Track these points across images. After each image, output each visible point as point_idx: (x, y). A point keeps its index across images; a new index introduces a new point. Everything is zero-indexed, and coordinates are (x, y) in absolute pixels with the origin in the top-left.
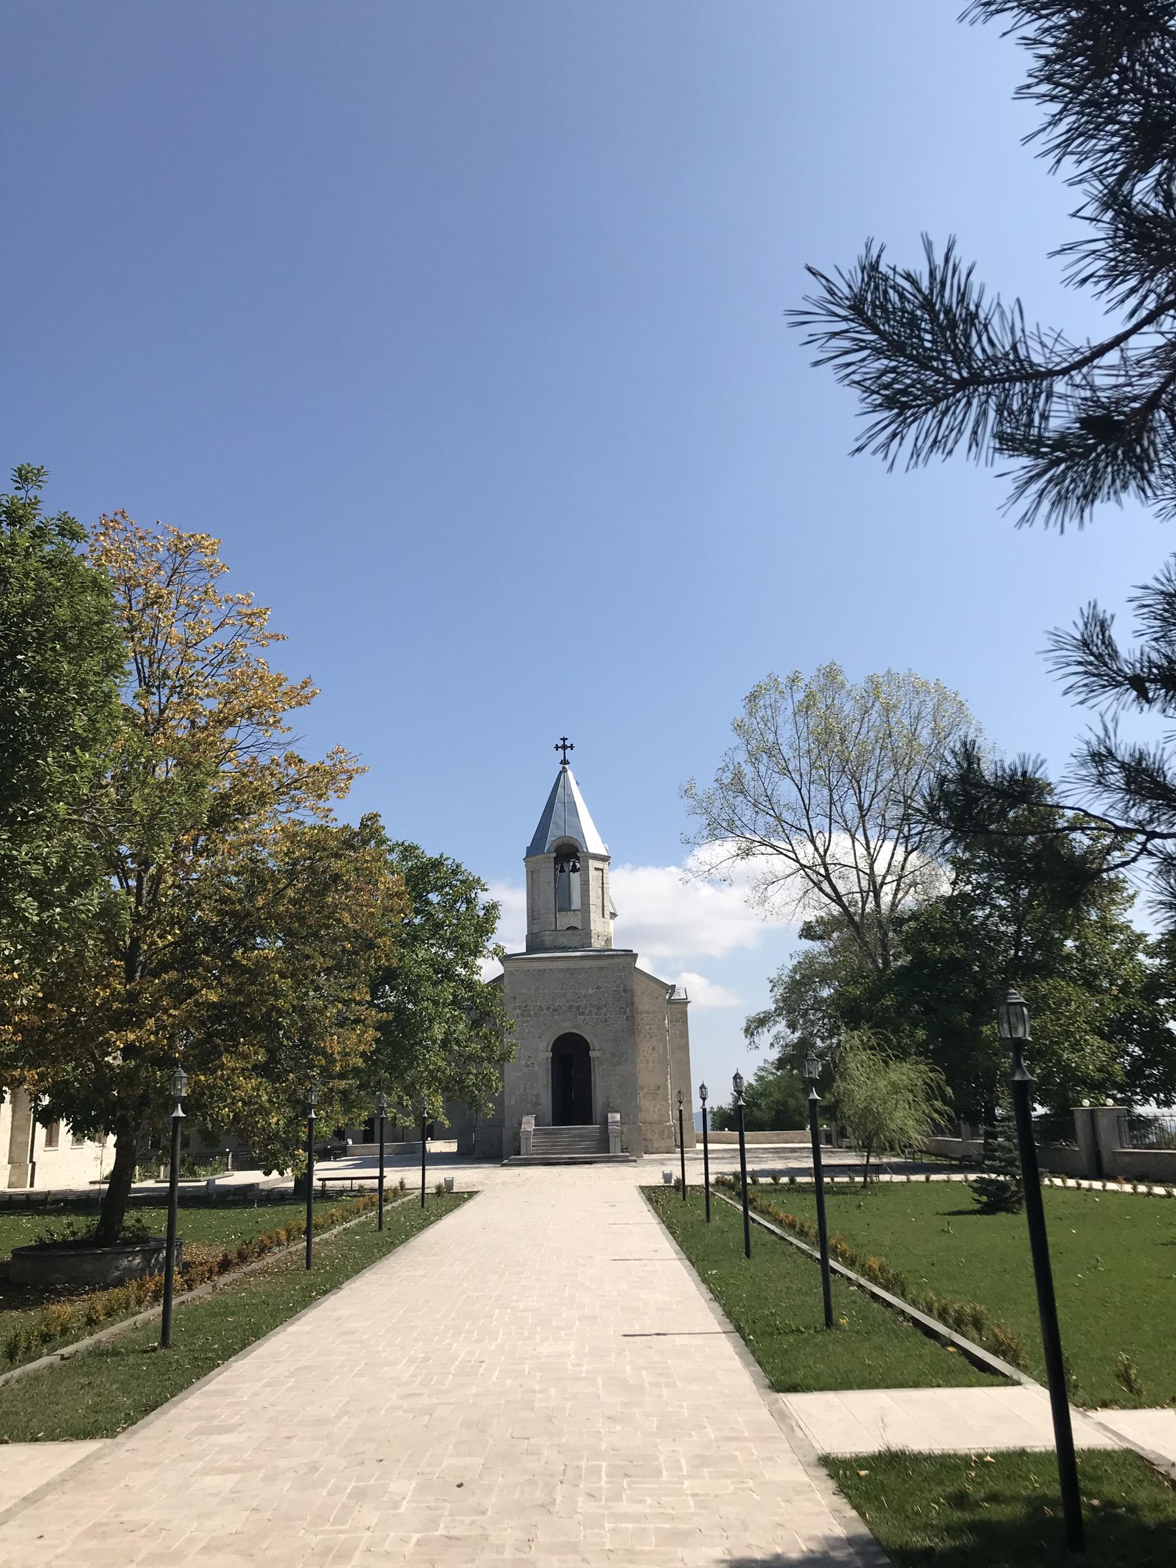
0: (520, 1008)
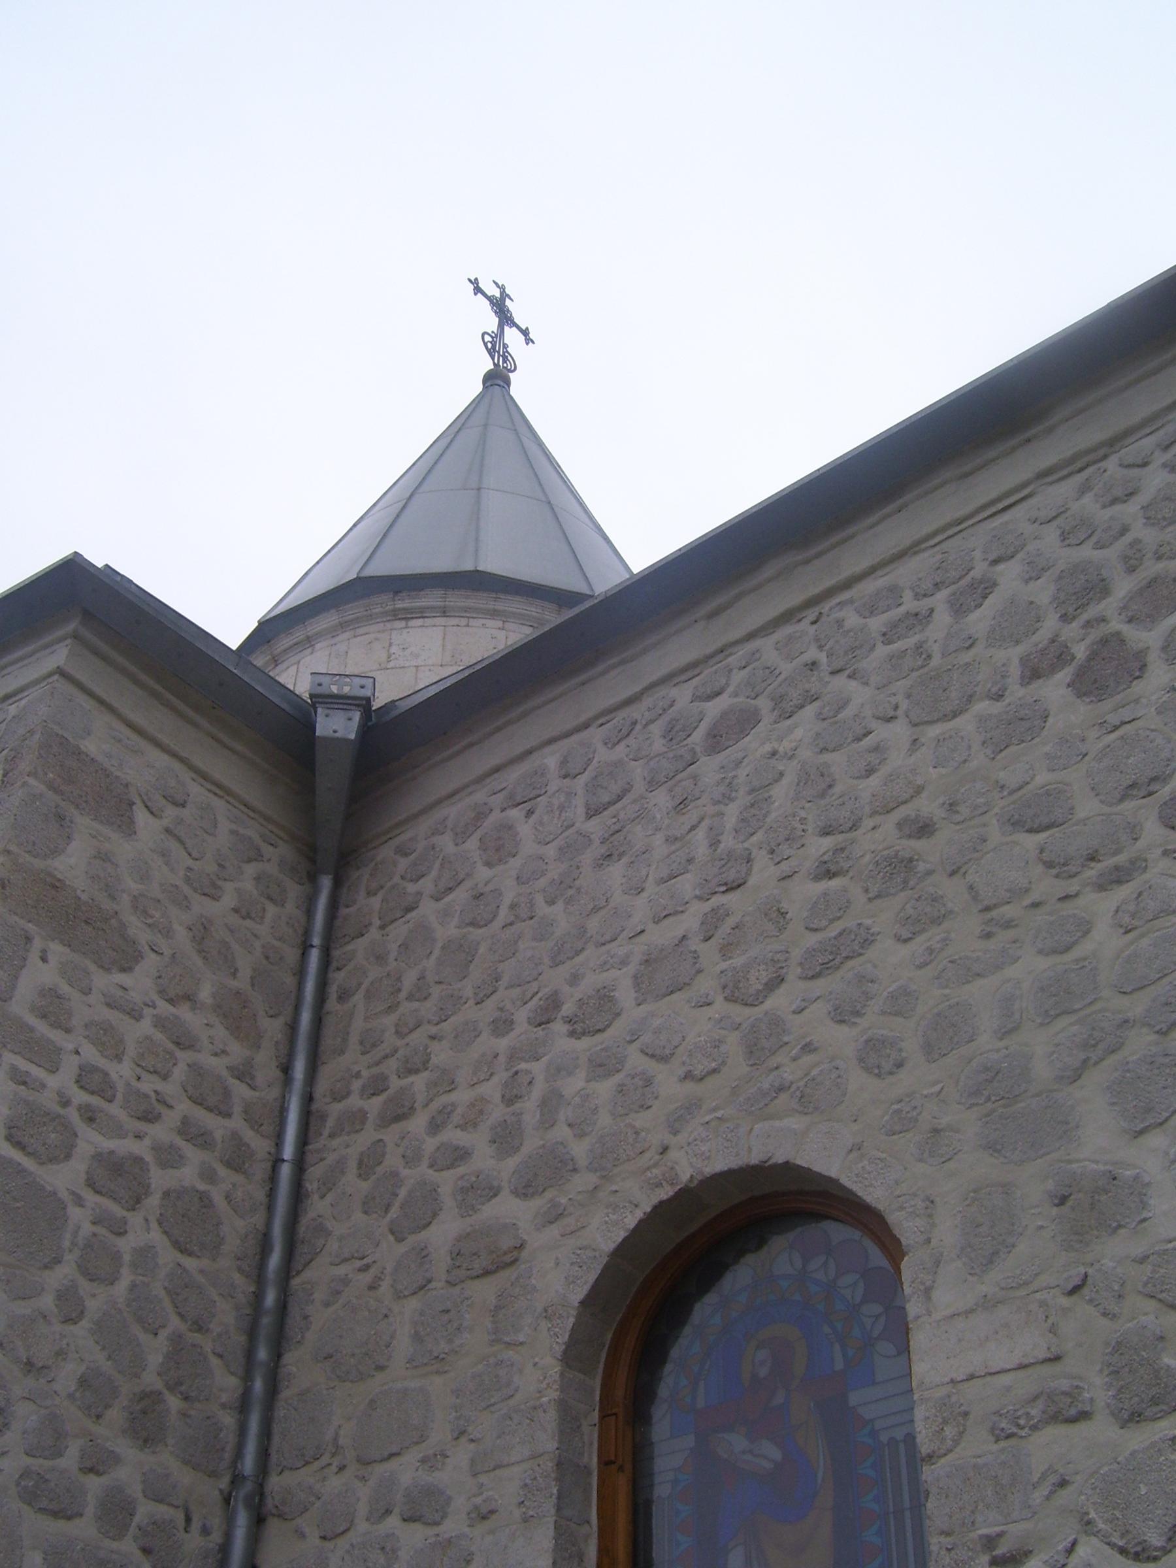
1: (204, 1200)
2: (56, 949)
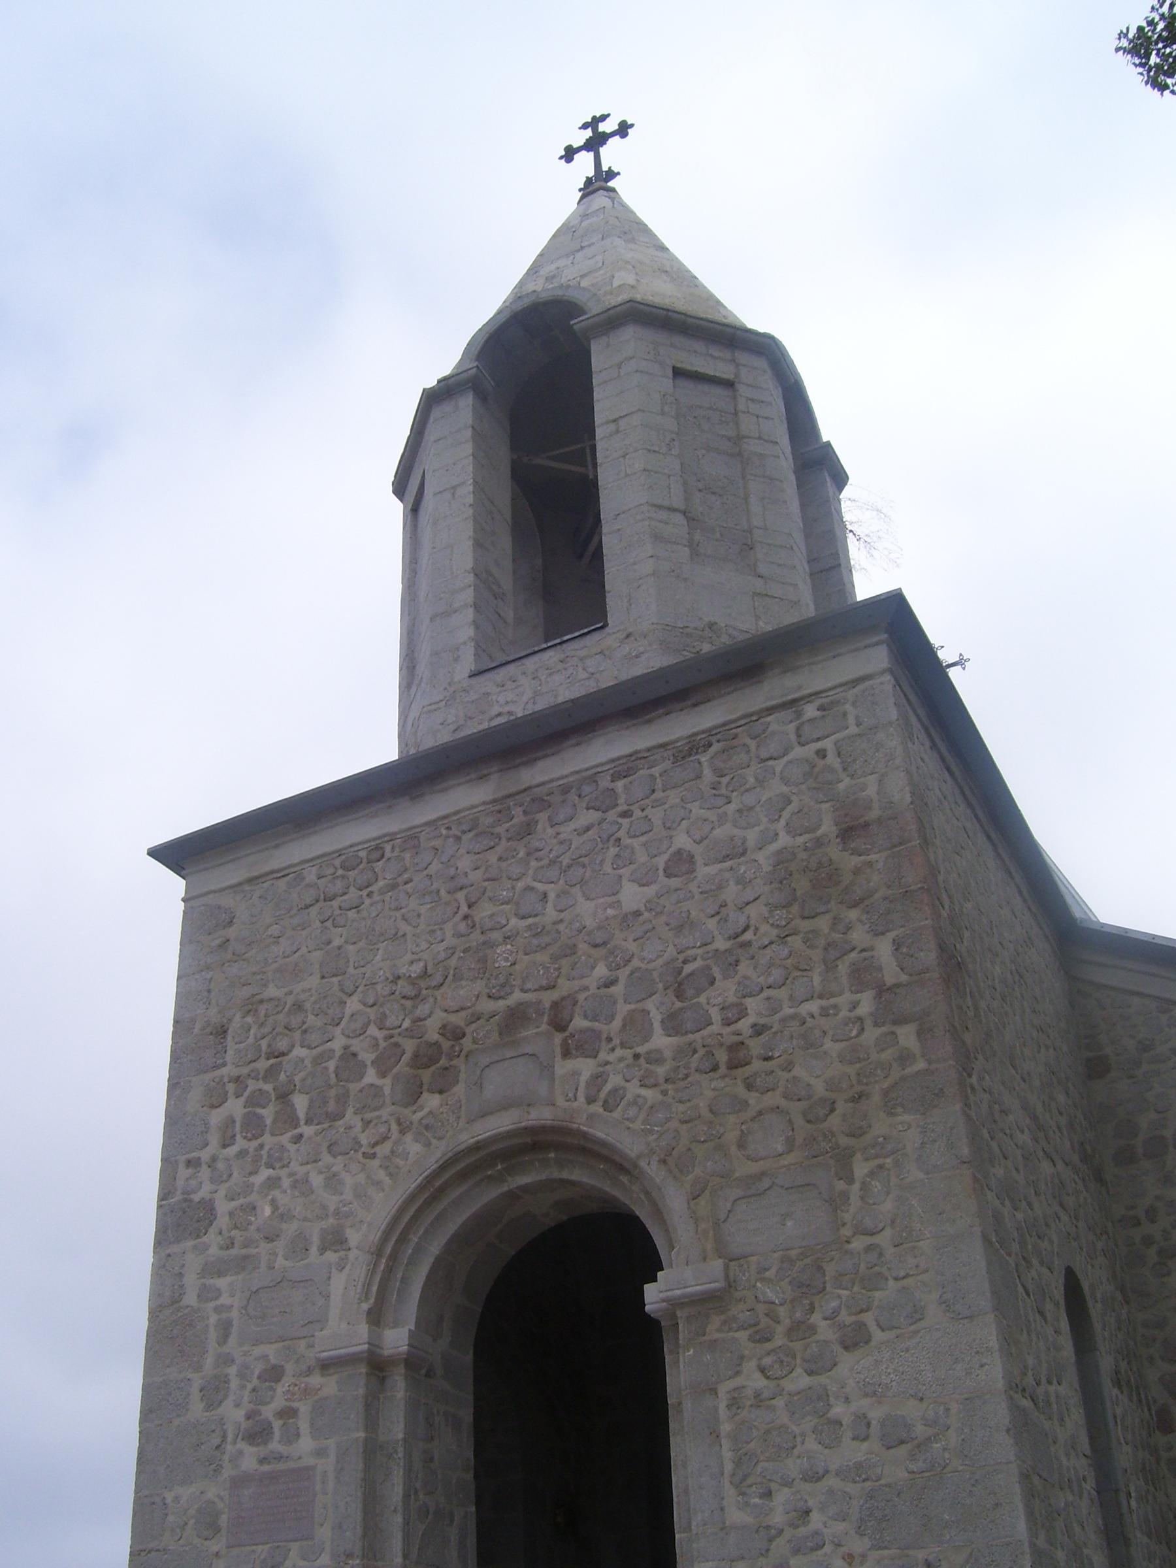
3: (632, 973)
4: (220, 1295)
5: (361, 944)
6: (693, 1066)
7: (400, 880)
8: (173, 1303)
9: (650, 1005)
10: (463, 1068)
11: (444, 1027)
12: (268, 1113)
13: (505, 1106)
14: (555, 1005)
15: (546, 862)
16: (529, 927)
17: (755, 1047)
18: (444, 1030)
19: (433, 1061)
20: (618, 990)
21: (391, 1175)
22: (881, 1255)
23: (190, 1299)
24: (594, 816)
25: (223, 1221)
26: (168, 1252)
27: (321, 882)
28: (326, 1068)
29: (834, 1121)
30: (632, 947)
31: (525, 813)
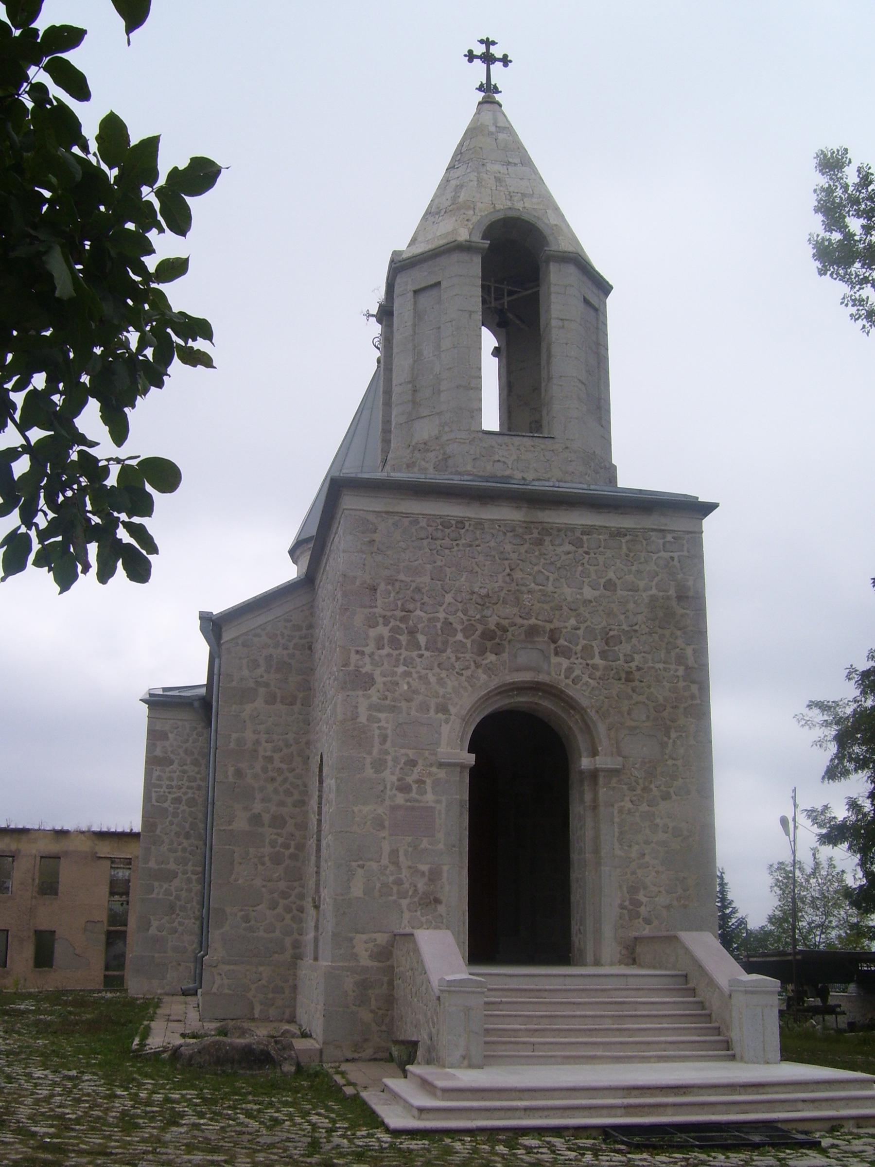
0: (386, 620)
1: (193, 798)
2: (158, 768)
3: (587, 627)
4: (381, 721)
5: (453, 569)
6: (611, 675)
7: (473, 543)
8: (352, 720)
9: (594, 643)
10: (507, 646)
11: (498, 624)
12: (404, 639)
13: (527, 669)
14: (551, 630)
15: (548, 562)
16: (540, 590)
17: (637, 675)
18: (498, 625)
19: (493, 638)
20: (580, 632)
21: (471, 686)
22: (678, 768)
23: (363, 719)
24: (571, 548)
25: (379, 685)
26: (348, 694)
27: (430, 529)
28: (436, 626)
29: (665, 714)
30: (587, 615)
31: (539, 533)
